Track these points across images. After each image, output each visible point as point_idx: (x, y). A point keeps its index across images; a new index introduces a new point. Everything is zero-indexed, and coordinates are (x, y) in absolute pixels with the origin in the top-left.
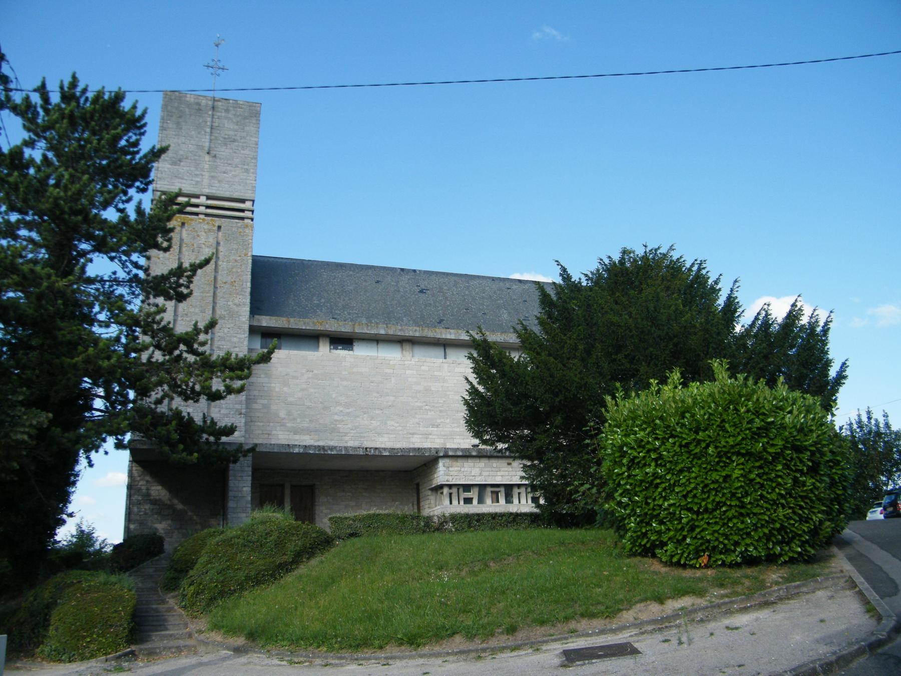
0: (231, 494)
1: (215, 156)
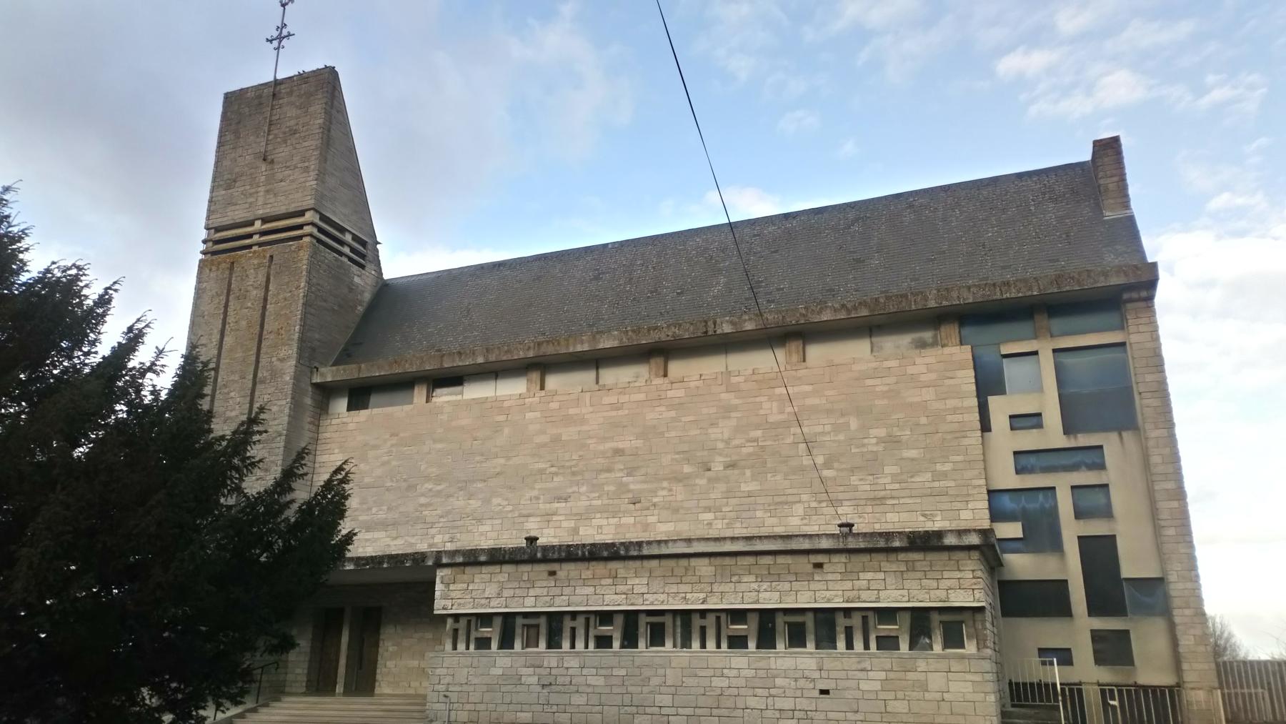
1: (272, 162)
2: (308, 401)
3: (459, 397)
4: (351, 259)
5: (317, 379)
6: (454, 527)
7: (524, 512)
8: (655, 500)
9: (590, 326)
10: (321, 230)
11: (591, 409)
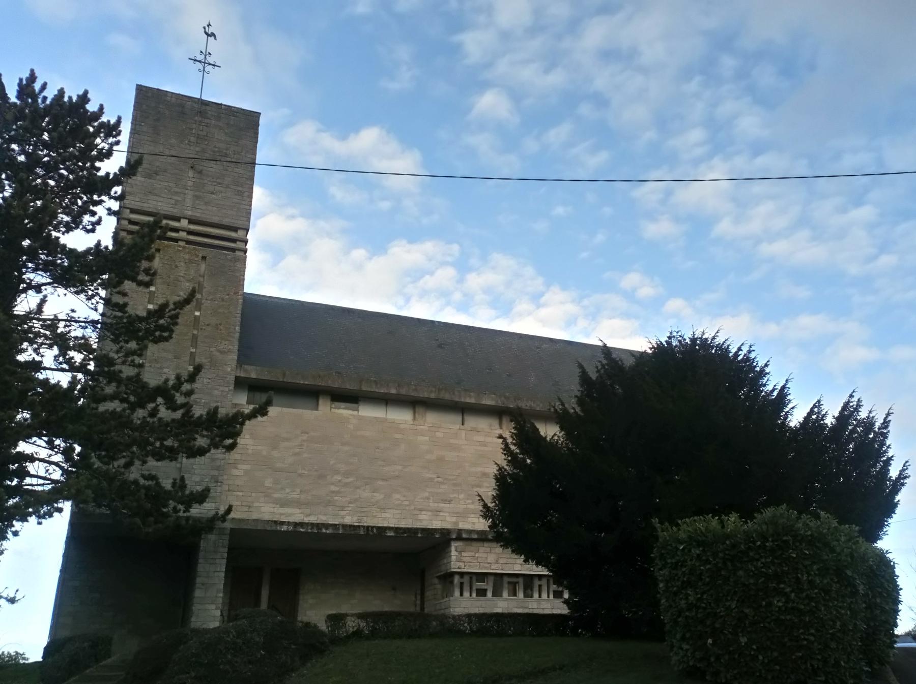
0: (199, 580)
3: (355, 413)
6: (361, 512)
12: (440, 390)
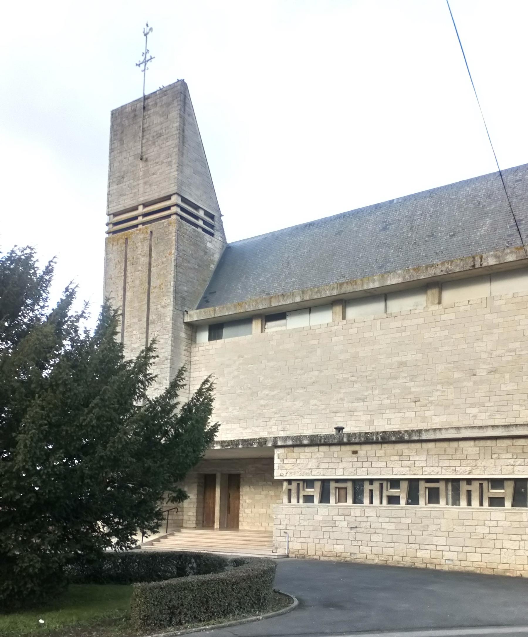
2: (183, 335)
4: (204, 230)
5: (187, 319)
6: (284, 421)
7: (334, 410)
8: (431, 399)
9: (380, 268)
10: (183, 209)
11: (381, 332)
12: (341, 285)
